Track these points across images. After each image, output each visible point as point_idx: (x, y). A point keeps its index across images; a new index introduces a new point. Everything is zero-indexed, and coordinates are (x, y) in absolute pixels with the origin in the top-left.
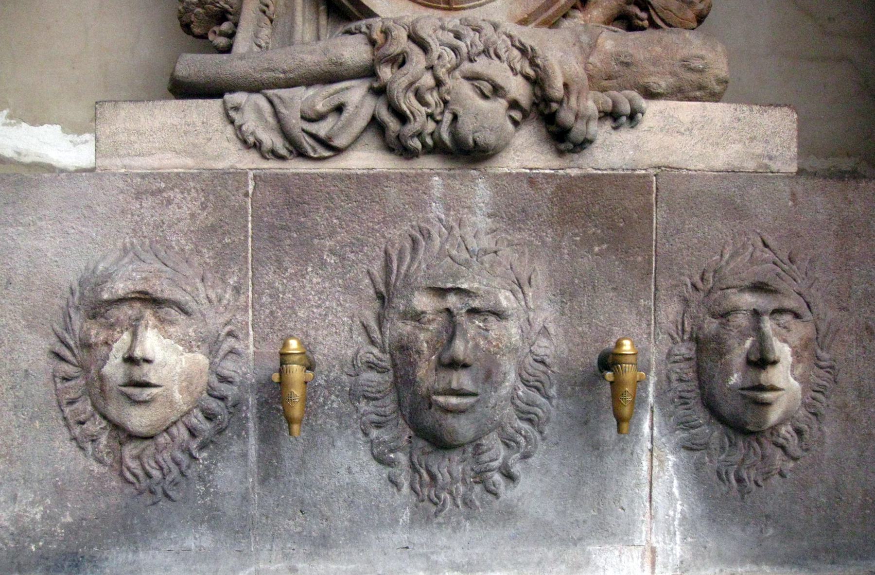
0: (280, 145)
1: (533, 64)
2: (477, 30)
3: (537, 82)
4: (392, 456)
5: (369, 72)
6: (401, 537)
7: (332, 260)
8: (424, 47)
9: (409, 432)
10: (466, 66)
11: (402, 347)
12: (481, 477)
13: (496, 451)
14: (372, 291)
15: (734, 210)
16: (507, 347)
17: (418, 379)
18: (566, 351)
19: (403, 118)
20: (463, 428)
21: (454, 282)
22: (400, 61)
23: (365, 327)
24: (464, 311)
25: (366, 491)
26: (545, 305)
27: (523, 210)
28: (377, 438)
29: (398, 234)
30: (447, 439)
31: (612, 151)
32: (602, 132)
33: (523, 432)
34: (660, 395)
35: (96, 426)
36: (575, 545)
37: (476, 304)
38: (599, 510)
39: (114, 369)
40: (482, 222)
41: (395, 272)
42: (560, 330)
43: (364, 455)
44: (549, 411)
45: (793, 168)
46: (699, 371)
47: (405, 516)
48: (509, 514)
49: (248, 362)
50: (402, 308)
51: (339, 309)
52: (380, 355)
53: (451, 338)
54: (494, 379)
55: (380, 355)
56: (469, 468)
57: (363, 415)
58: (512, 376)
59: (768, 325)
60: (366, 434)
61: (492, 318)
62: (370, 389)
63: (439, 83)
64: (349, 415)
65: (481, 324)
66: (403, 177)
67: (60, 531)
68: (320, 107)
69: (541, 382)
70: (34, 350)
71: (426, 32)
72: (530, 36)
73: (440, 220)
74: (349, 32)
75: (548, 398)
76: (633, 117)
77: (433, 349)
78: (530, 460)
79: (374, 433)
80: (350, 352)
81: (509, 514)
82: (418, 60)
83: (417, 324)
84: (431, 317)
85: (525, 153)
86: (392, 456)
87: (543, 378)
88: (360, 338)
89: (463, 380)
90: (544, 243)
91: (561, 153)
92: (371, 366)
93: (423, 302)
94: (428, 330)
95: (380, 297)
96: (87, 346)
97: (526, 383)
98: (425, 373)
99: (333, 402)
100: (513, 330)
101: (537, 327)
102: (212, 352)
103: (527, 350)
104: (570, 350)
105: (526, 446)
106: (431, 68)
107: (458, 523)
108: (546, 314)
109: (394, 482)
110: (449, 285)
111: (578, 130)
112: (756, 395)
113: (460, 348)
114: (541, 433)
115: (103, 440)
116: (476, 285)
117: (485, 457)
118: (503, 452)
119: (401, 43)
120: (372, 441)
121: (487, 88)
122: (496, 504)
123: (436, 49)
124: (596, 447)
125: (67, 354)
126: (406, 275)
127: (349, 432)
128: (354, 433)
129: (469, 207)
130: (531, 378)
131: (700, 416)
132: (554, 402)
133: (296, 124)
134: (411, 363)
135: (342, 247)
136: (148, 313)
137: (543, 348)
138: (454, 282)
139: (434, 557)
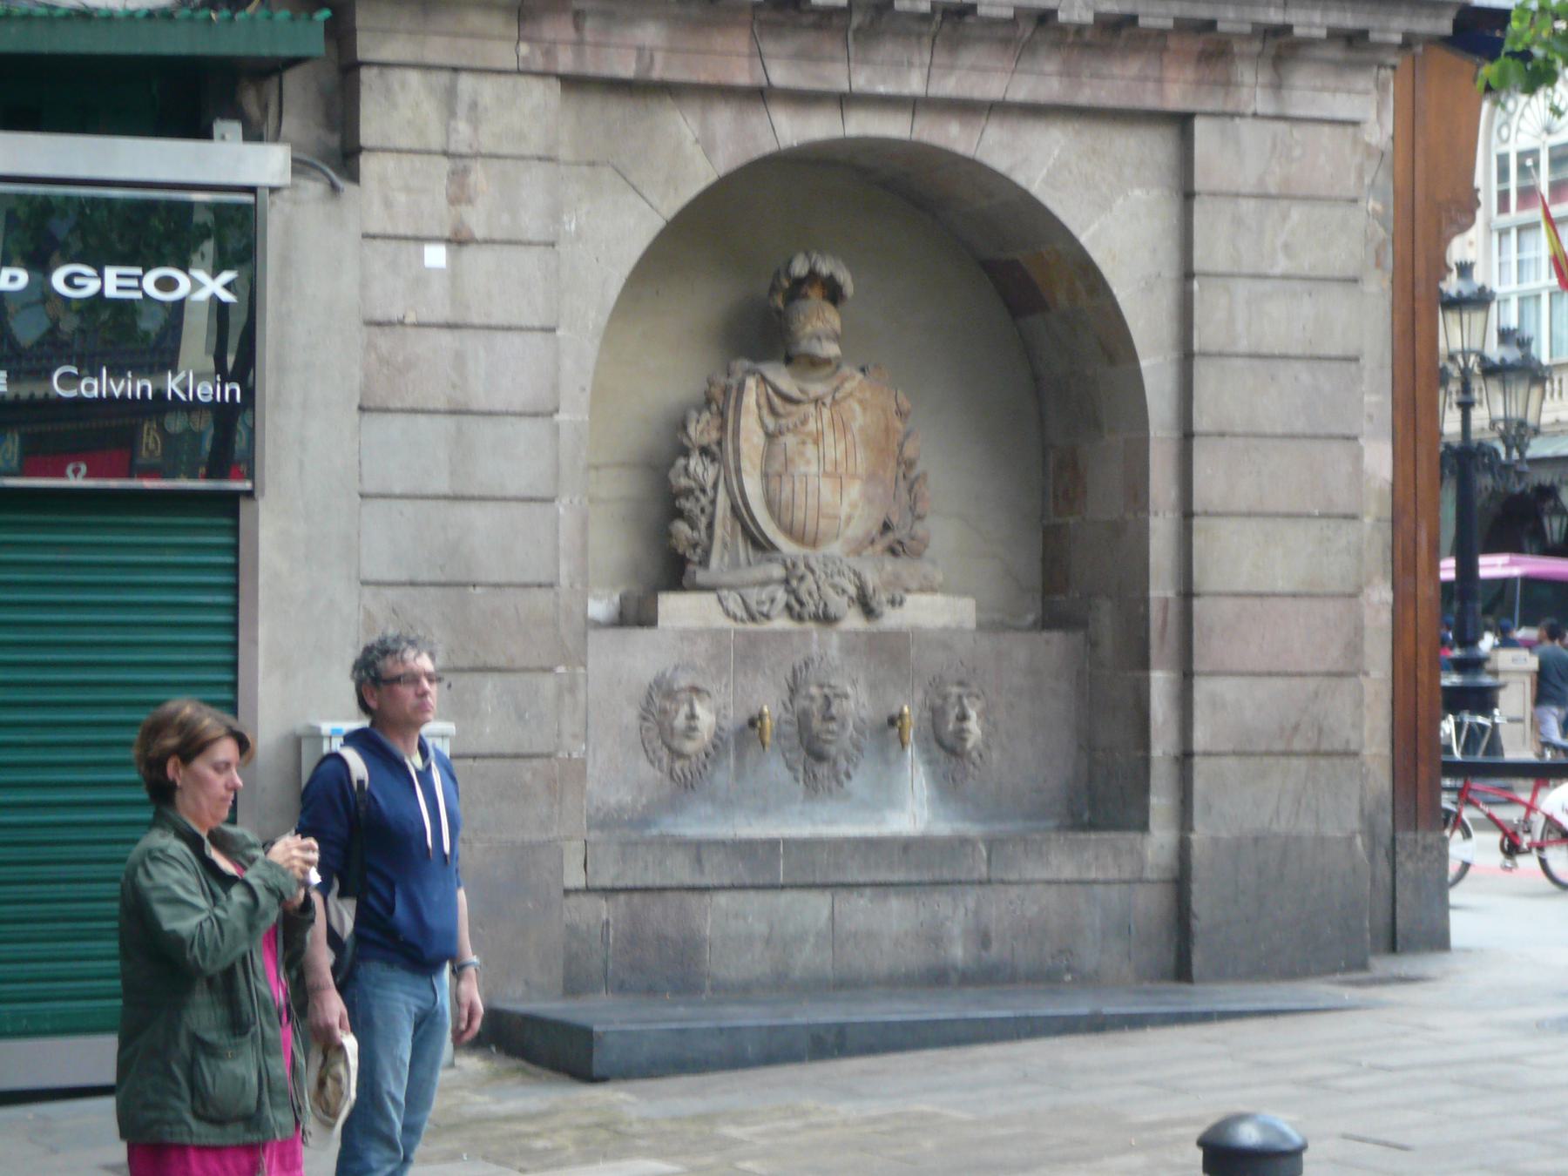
0: (745, 616)
3: (861, 588)
5: (786, 581)
8: (812, 572)
9: (804, 754)
13: (842, 764)
19: (801, 604)
20: (832, 750)
22: (802, 578)
29: (798, 660)
31: (892, 619)
34: (915, 737)
39: (680, 722)
40: (834, 652)
43: (782, 764)
46: (934, 725)
47: (801, 797)
48: (848, 796)
49: (735, 717)
59: (966, 701)
70: (631, 716)
71: (813, 563)
72: (854, 562)
74: (770, 560)
76: (901, 603)
81: (848, 796)
82: (810, 578)
85: (853, 621)
89: (833, 726)
93: (814, 690)
95: (792, 691)
96: (664, 712)
98: (816, 724)
108: (864, 697)
109: (796, 780)
111: (878, 609)
112: (961, 735)
115: (665, 760)
124: (886, 762)
131: (934, 746)
133: (754, 607)
137: (863, 713)
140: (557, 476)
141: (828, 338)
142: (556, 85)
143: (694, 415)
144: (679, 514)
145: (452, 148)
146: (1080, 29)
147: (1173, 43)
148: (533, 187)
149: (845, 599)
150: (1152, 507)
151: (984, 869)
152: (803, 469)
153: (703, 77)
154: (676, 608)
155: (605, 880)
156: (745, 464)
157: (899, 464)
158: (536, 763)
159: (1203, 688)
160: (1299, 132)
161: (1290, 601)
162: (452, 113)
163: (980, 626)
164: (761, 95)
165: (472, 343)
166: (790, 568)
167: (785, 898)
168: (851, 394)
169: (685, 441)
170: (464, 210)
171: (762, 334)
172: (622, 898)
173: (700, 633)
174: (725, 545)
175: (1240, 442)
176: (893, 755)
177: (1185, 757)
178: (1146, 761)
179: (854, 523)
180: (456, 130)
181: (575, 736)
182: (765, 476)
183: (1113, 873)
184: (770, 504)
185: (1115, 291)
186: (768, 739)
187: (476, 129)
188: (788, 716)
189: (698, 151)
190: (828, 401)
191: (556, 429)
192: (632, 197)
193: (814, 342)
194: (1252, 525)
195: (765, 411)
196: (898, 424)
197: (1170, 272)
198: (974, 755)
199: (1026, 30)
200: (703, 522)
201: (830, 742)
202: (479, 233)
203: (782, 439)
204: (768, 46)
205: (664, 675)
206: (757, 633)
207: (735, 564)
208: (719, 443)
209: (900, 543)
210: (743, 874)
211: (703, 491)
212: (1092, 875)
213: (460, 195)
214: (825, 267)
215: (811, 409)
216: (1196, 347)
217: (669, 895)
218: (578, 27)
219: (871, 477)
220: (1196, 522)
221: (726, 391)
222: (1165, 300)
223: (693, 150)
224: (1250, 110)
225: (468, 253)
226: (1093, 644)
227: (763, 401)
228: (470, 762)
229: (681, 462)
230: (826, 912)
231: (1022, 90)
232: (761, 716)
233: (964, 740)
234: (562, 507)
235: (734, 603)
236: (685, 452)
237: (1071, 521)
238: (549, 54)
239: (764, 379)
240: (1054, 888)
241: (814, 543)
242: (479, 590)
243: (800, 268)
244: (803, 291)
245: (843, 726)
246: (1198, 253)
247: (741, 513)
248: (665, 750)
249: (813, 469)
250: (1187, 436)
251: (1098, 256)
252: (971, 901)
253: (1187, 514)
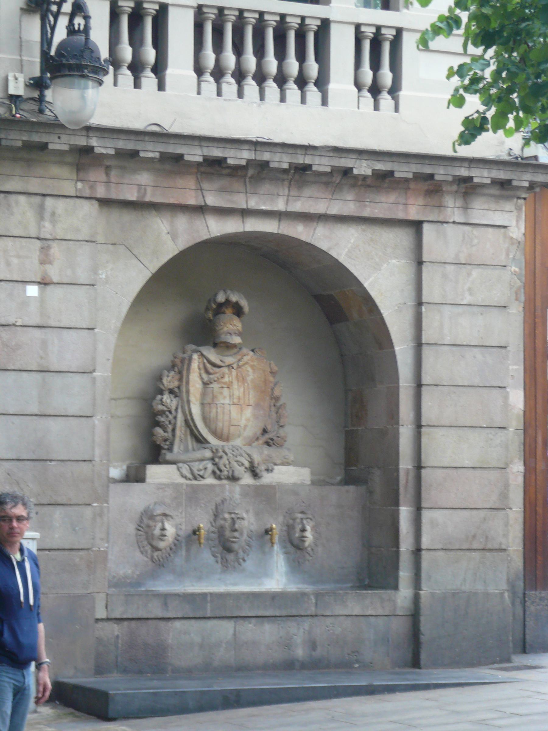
1: (251, 458)
2: (237, 450)
3: (251, 463)
5: (212, 459)
7: (203, 506)
9: (221, 548)
10: (236, 459)
13: (241, 554)
15: (296, 493)
19: (220, 471)
20: (235, 546)
22: (221, 458)
29: (218, 500)
31: (267, 479)
32: (265, 474)
35: (148, 548)
37: (239, 516)
39: (157, 532)
40: (237, 496)
45: (309, 483)
47: (219, 570)
59: (305, 522)
60: (211, 549)
63: (230, 463)
66: (220, 485)
67: (135, 576)
68: (201, 467)
70: (131, 528)
72: (247, 449)
74: (205, 448)
76: (272, 471)
79: (213, 549)
82: (225, 457)
85: (247, 480)
88: (209, 525)
89: (236, 534)
91: (255, 479)
92: (213, 532)
96: (149, 526)
98: (228, 533)
102: (176, 528)
106: (228, 459)
108: (252, 520)
109: (217, 562)
111: (260, 474)
112: (302, 539)
115: (149, 551)
119: (221, 453)
121: (240, 464)
123: (230, 455)
125: (141, 529)
131: (289, 545)
133: (196, 472)
136: (164, 518)
137: (253, 528)
140: (94, 405)
141: (235, 333)
142: (96, 203)
143: (166, 373)
144: (158, 424)
145: (42, 236)
146: (365, 177)
147: (412, 185)
148: (83, 256)
149: (243, 467)
150: (401, 422)
151: (313, 609)
152: (222, 401)
153: (172, 201)
154: (156, 473)
155: (117, 614)
156: (192, 399)
157: (271, 399)
158: (81, 553)
159: (426, 515)
160: (476, 231)
161: (471, 471)
162: (42, 218)
163: (313, 483)
164: (201, 210)
165: (50, 335)
166: (215, 452)
167: (210, 624)
168: (247, 363)
169: (162, 387)
170: (47, 267)
171: (202, 331)
172: (126, 623)
173: (167, 485)
174: (181, 440)
175: (446, 389)
176: (267, 550)
177: (417, 551)
178: (397, 553)
179: (248, 429)
180: (44, 227)
181: (102, 539)
182: (202, 404)
183: (380, 612)
184: (205, 419)
185: (382, 311)
186: (202, 541)
187: (54, 226)
188: (213, 529)
189: (169, 238)
190: (235, 366)
191: (94, 380)
192: (134, 261)
193: (228, 336)
194: (452, 431)
195: (203, 371)
196: (271, 379)
197: (411, 302)
198: (309, 549)
199: (337, 178)
200: (170, 428)
202: (55, 279)
203: (211, 386)
204: (206, 185)
205: (149, 507)
206: (198, 486)
207: (186, 450)
208: (179, 387)
209: (272, 439)
210: (188, 611)
211: (170, 412)
212: (369, 612)
213: (45, 260)
214: (234, 298)
215: (226, 370)
216: (423, 341)
217: (150, 622)
218: (107, 174)
219: (257, 406)
220: (423, 430)
221: (183, 361)
222: (408, 316)
223: (167, 238)
224: (451, 221)
225: (50, 288)
226: (371, 492)
227: (201, 366)
228: (47, 552)
229: (159, 397)
230: (231, 631)
231: (335, 209)
232: (199, 529)
233: (304, 541)
234: (96, 420)
235: (185, 470)
236: (161, 392)
237: (360, 428)
238: (92, 188)
239: (202, 355)
240: (349, 618)
241: (227, 440)
242: (53, 463)
243: (221, 298)
244: (222, 310)
245: (241, 534)
246: (425, 293)
247: (189, 424)
248: (149, 546)
249: (227, 401)
250: (419, 385)
251: (373, 294)
252: (306, 626)
253: (419, 426)
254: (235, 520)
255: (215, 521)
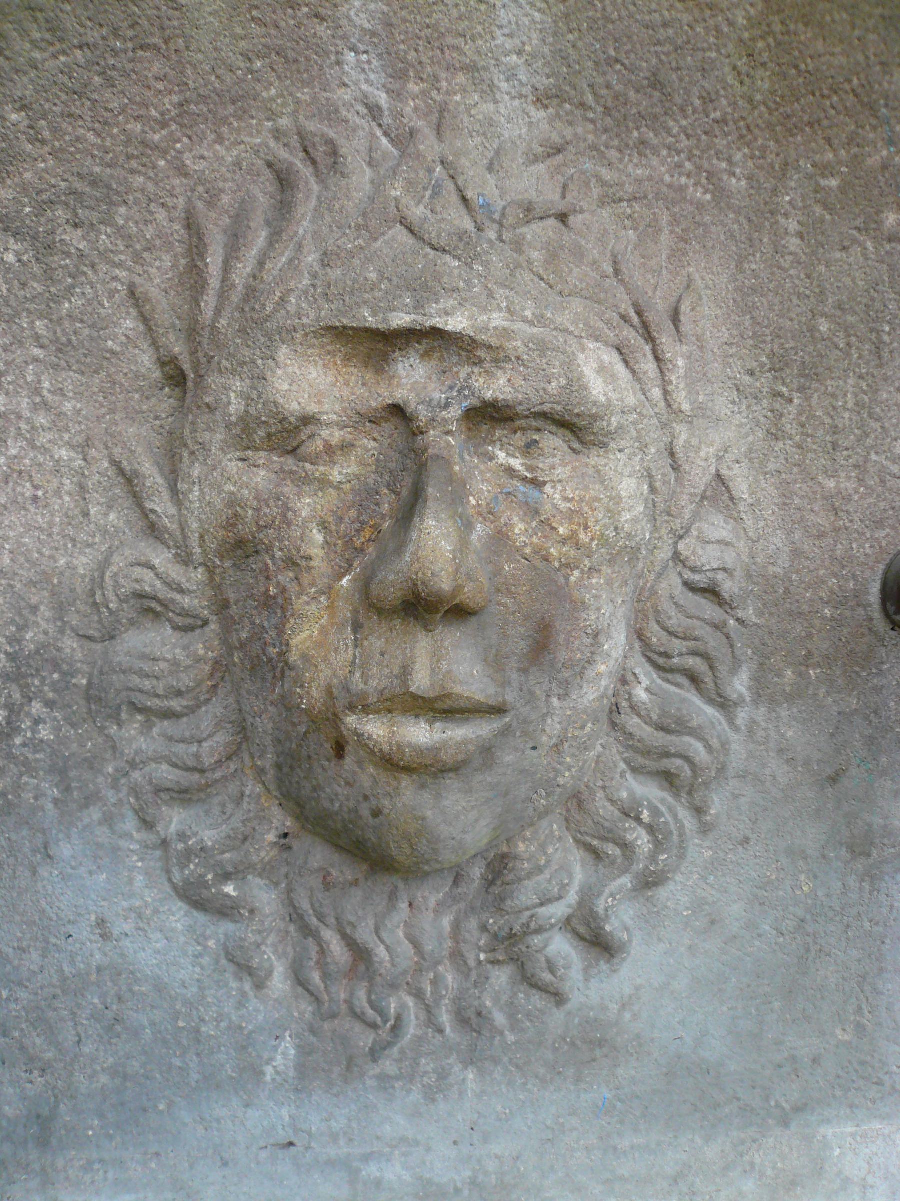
4: (230, 889)
6: (275, 1115)
9: (281, 819)
11: (240, 543)
12: (512, 946)
13: (557, 874)
14: (146, 360)
16: (604, 541)
17: (294, 657)
18: (784, 560)
20: (459, 818)
21: (418, 306)
23: (129, 480)
24: (455, 412)
25: (160, 988)
26: (722, 405)
27: (656, 82)
28: (182, 836)
30: (399, 852)
33: (646, 815)
36: (785, 1123)
37: (498, 387)
38: (860, 1028)
41: (214, 283)
42: (770, 489)
44: (725, 744)
47: (284, 1055)
50: (236, 406)
51: (42, 420)
52: (176, 573)
53: (409, 511)
54: (563, 655)
55: (176, 573)
56: (473, 923)
57: (133, 764)
58: (617, 641)
60: (148, 824)
61: (553, 442)
62: (147, 684)
64: (92, 763)
65: (517, 463)
69: (704, 655)
73: (374, 111)
75: (724, 704)
77: (347, 551)
78: (662, 893)
79: (174, 819)
80: (84, 562)
81: (593, 1045)
83: (290, 463)
84: (336, 436)
86: (230, 889)
87: (713, 642)
89: (450, 660)
90: (720, 193)
92: (150, 607)
93: (310, 383)
94: (324, 483)
95: (176, 378)
97: (660, 661)
98: (319, 638)
99: (37, 721)
100: (622, 481)
101: (699, 476)
103: (664, 554)
104: (797, 553)
105: (653, 857)
107: (443, 1075)
108: (725, 435)
109: (242, 964)
110: (401, 320)
113: (438, 548)
114: (699, 811)
116: (498, 319)
117: (525, 895)
118: (579, 872)
120: (165, 843)
122: (557, 1018)
126: (251, 293)
127: (95, 813)
128: (108, 820)
129: (471, 68)
130: (677, 645)
132: (742, 716)
134: (267, 602)
135: (41, 209)
137: (716, 544)
138: (418, 306)
139: (372, 1170)
201: (429, 768)
245: (543, 645)
254: (447, 440)
255: (173, 455)
